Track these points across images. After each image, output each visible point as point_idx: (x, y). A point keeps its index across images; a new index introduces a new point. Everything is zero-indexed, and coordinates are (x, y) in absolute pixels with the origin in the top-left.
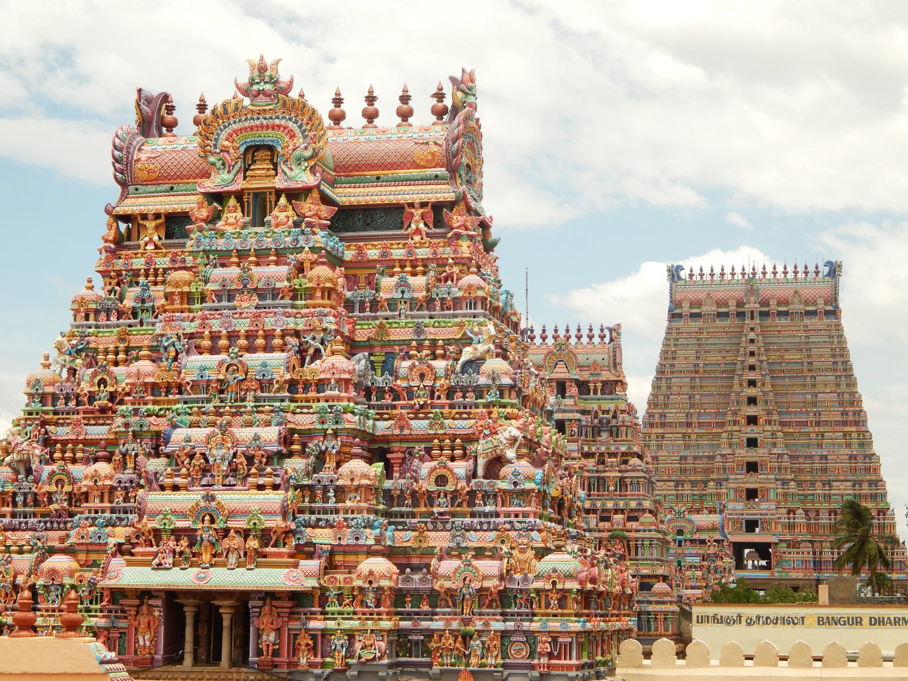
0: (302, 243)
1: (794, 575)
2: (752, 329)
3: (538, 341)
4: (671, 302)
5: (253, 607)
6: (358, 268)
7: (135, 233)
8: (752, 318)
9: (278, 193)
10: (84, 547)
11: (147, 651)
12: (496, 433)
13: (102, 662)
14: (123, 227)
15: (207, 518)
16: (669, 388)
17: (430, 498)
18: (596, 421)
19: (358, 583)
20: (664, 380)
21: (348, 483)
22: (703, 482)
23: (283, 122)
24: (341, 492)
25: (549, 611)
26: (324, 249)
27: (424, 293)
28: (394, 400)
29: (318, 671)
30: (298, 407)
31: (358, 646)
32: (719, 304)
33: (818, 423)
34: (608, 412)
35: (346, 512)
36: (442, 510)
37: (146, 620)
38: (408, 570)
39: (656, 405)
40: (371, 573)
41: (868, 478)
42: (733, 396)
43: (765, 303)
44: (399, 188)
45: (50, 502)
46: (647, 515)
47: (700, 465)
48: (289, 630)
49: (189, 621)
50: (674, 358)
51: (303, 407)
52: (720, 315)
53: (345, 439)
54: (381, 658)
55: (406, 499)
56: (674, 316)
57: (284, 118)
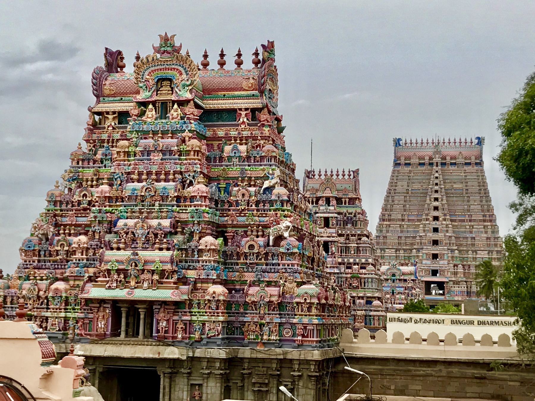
0: (184, 128)
1: (456, 298)
2: (437, 172)
3: (317, 177)
5: (156, 309)
6: (214, 141)
7: (103, 122)
8: (437, 166)
9: (174, 102)
10: (73, 278)
11: (102, 330)
12: (279, 224)
13: (34, 333)
14: (97, 118)
15: (134, 264)
16: (393, 201)
17: (246, 256)
18: (345, 218)
19: (207, 297)
20: (390, 197)
21: (204, 247)
22: (409, 249)
23: (176, 67)
24: (200, 252)
25: (303, 313)
26: (196, 131)
27: (246, 154)
28: (229, 207)
29: (187, 341)
30: (181, 210)
31: (207, 329)
32: (420, 158)
33: (470, 221)
34: (351, 213)
35: (203, 262)
36: (251, 262)
37: (102, 314)
38: (233, 292)
39: (386, 210)
40: (214, 293)
41: (496, 249)
42: (426, 206)
43: (444, 158)
44: (235, 101)
45: (57, 255)
46: (371, 266)
47: (409, 241)
48: (173, 320)
49: (124, 315)
50: (396, 186)
51: (184, 210)
52: (420, 164)
53: (203, 226)
54: (218, 335)
55: (234, 256)
57: (176, 65)
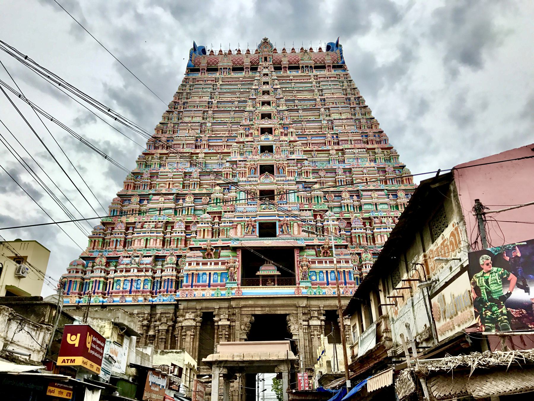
4: (191, 60)
41: (403, 187)
52: (235, 69)
56: (192, 69)
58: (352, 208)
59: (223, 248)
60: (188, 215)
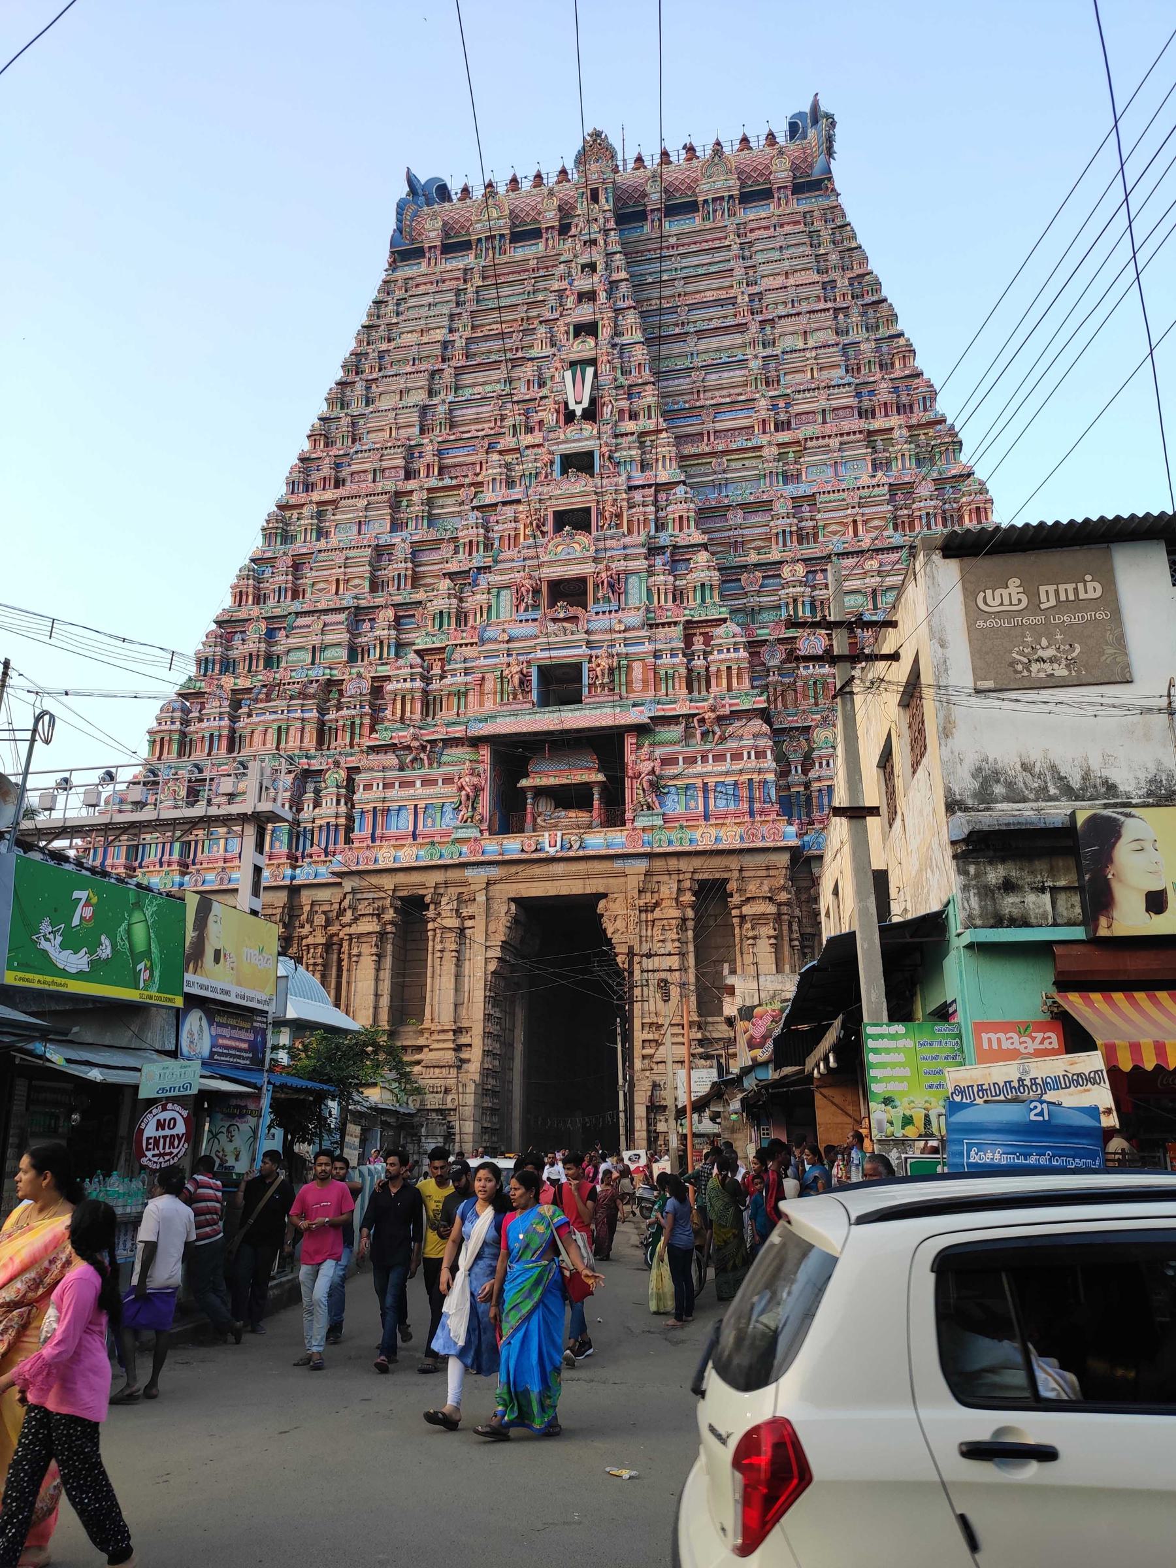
1: (704, 837)
4: (399, 230)
56: (405, 252)
58: (808, 608)
59: (450, 742)
60: (380, 658)
